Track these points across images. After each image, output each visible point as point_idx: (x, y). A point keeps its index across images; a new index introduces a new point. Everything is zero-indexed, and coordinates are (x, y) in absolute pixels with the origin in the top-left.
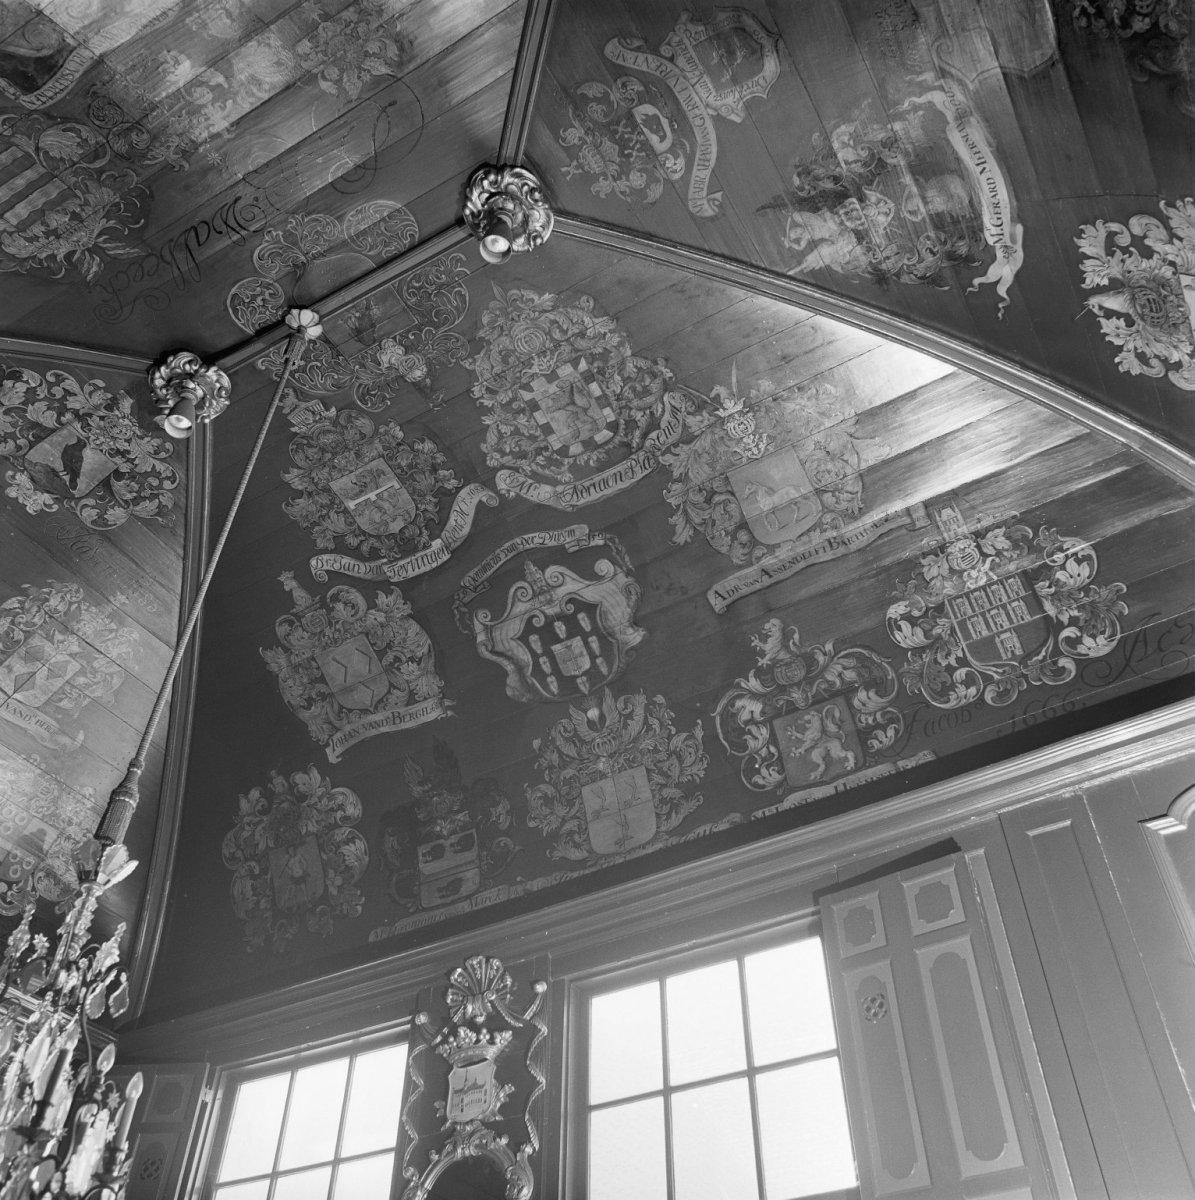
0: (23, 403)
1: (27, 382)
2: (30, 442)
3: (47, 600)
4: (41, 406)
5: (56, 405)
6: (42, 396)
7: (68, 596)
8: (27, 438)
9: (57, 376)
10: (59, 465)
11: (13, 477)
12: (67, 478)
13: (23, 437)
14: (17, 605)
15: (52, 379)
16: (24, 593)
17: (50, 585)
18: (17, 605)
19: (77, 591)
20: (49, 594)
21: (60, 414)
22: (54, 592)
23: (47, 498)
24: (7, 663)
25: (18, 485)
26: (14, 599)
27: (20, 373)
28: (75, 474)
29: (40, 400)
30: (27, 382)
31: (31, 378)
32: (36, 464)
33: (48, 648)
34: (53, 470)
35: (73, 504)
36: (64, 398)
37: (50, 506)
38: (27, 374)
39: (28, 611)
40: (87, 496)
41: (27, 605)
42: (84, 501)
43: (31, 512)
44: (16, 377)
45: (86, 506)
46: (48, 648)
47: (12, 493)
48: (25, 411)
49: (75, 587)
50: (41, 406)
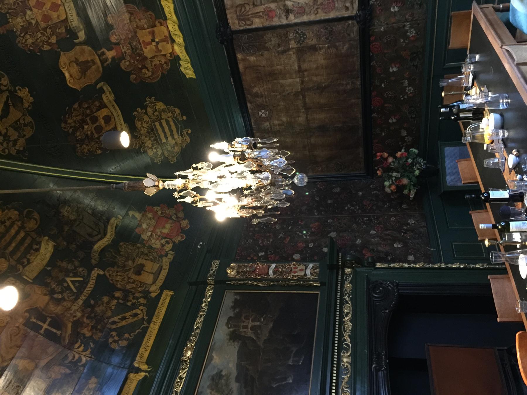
0: (18, 140)
1: (15, 149)
2: (19, 121)
3: (32, 43)
4: (12, 138)
5: (7, 138)
6: (11, 143)
7: (23, 41)
8: (20, 123)
9: (4, 152)
10: (12, 108)
11: (29, 106)
12: (10, 102)
13: (21, 124)
14: (45, 46)
15: (7, 151)
16: (41, 51)
17: (30, 50)
18: (45, 46)
19: (19, 42)
20: (31, 46)
21: (6, 134)
22: (29, 46)
23: (20, 94)
24: (58, 21)
25: (28, 102)
26: (45, 49)
27: (17, 153)
28: (6, 105)
29: (12, 141)
30: (15, 149)
31: (13, 152)
32: (19, 111)
33: (39, 19)
34: (14, 107)
35: (10, 88)
36: (4, 141)
37: (19, 89)
38: (13, 152)
39: (41, 41)
40: (4, 91)
41: (41, 44)
42: (5, 88)
43: (27, 89)
44: (18, 152)
45: (5, 86)
46: (39, 19)
47: (31, 99)
48: (18, 136)
49: (20, 45)
50: (12, 138)
